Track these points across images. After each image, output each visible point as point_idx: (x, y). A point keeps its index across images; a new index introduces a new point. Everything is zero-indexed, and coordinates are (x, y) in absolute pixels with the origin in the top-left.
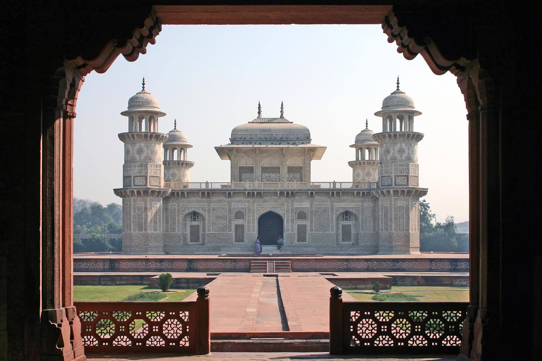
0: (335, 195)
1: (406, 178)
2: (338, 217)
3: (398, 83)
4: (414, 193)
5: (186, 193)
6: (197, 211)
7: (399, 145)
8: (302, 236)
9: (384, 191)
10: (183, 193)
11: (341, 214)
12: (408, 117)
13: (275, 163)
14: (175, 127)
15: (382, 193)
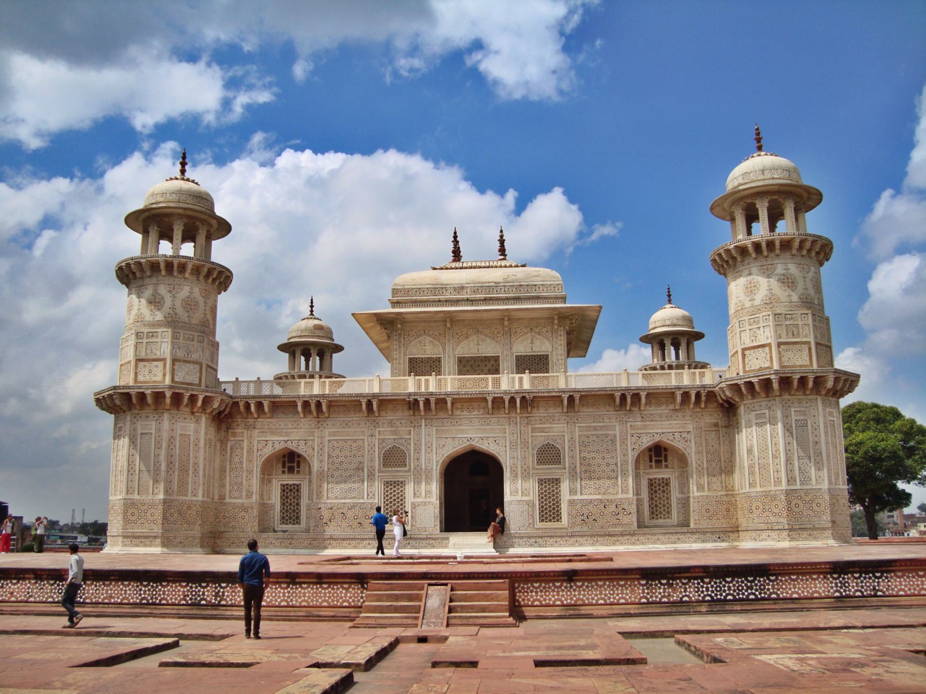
0: (629, 400)
1: (806, 347)
2: (637, 461)
3: (759, 140)
4: (830, 384)
5: (266, 404)
6: (292, 446)
7: (780, 269)
8: (549, 510)
9: (755, 380)
10: (260, 405)
11: (643, 452)
12: (793, 206)
13: (488, 348)
14: (312, 311)
15: (750, 385)
